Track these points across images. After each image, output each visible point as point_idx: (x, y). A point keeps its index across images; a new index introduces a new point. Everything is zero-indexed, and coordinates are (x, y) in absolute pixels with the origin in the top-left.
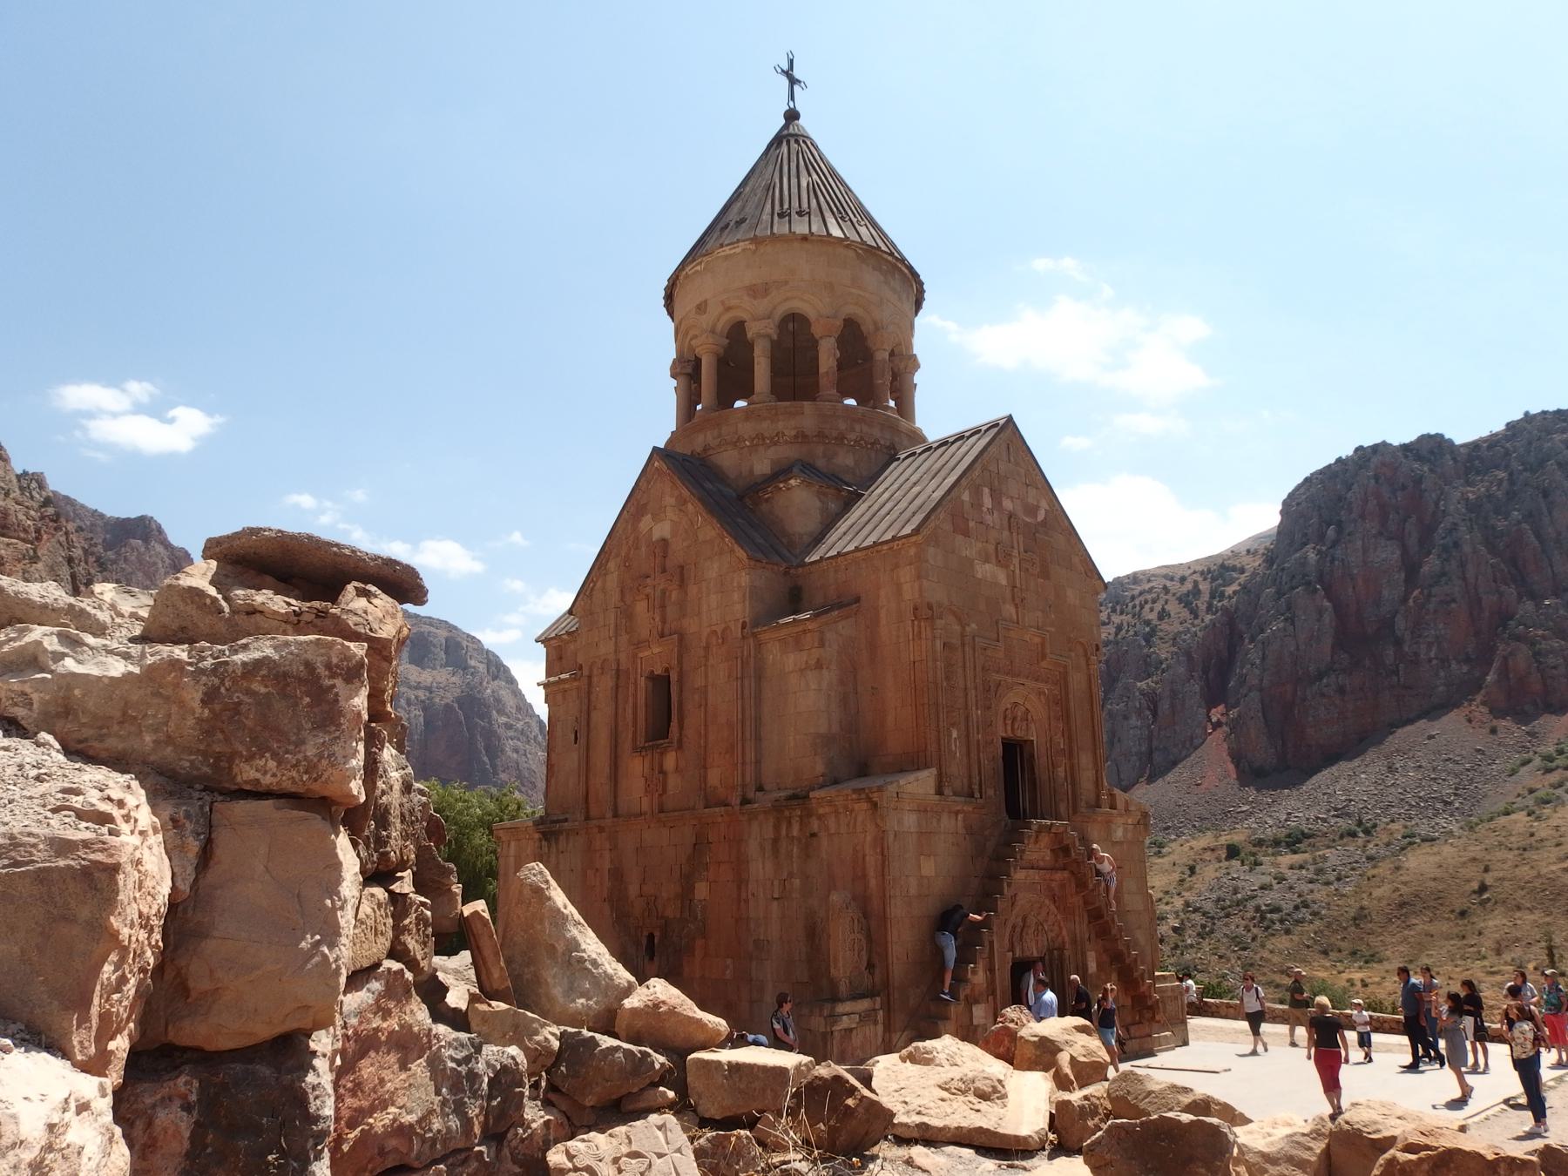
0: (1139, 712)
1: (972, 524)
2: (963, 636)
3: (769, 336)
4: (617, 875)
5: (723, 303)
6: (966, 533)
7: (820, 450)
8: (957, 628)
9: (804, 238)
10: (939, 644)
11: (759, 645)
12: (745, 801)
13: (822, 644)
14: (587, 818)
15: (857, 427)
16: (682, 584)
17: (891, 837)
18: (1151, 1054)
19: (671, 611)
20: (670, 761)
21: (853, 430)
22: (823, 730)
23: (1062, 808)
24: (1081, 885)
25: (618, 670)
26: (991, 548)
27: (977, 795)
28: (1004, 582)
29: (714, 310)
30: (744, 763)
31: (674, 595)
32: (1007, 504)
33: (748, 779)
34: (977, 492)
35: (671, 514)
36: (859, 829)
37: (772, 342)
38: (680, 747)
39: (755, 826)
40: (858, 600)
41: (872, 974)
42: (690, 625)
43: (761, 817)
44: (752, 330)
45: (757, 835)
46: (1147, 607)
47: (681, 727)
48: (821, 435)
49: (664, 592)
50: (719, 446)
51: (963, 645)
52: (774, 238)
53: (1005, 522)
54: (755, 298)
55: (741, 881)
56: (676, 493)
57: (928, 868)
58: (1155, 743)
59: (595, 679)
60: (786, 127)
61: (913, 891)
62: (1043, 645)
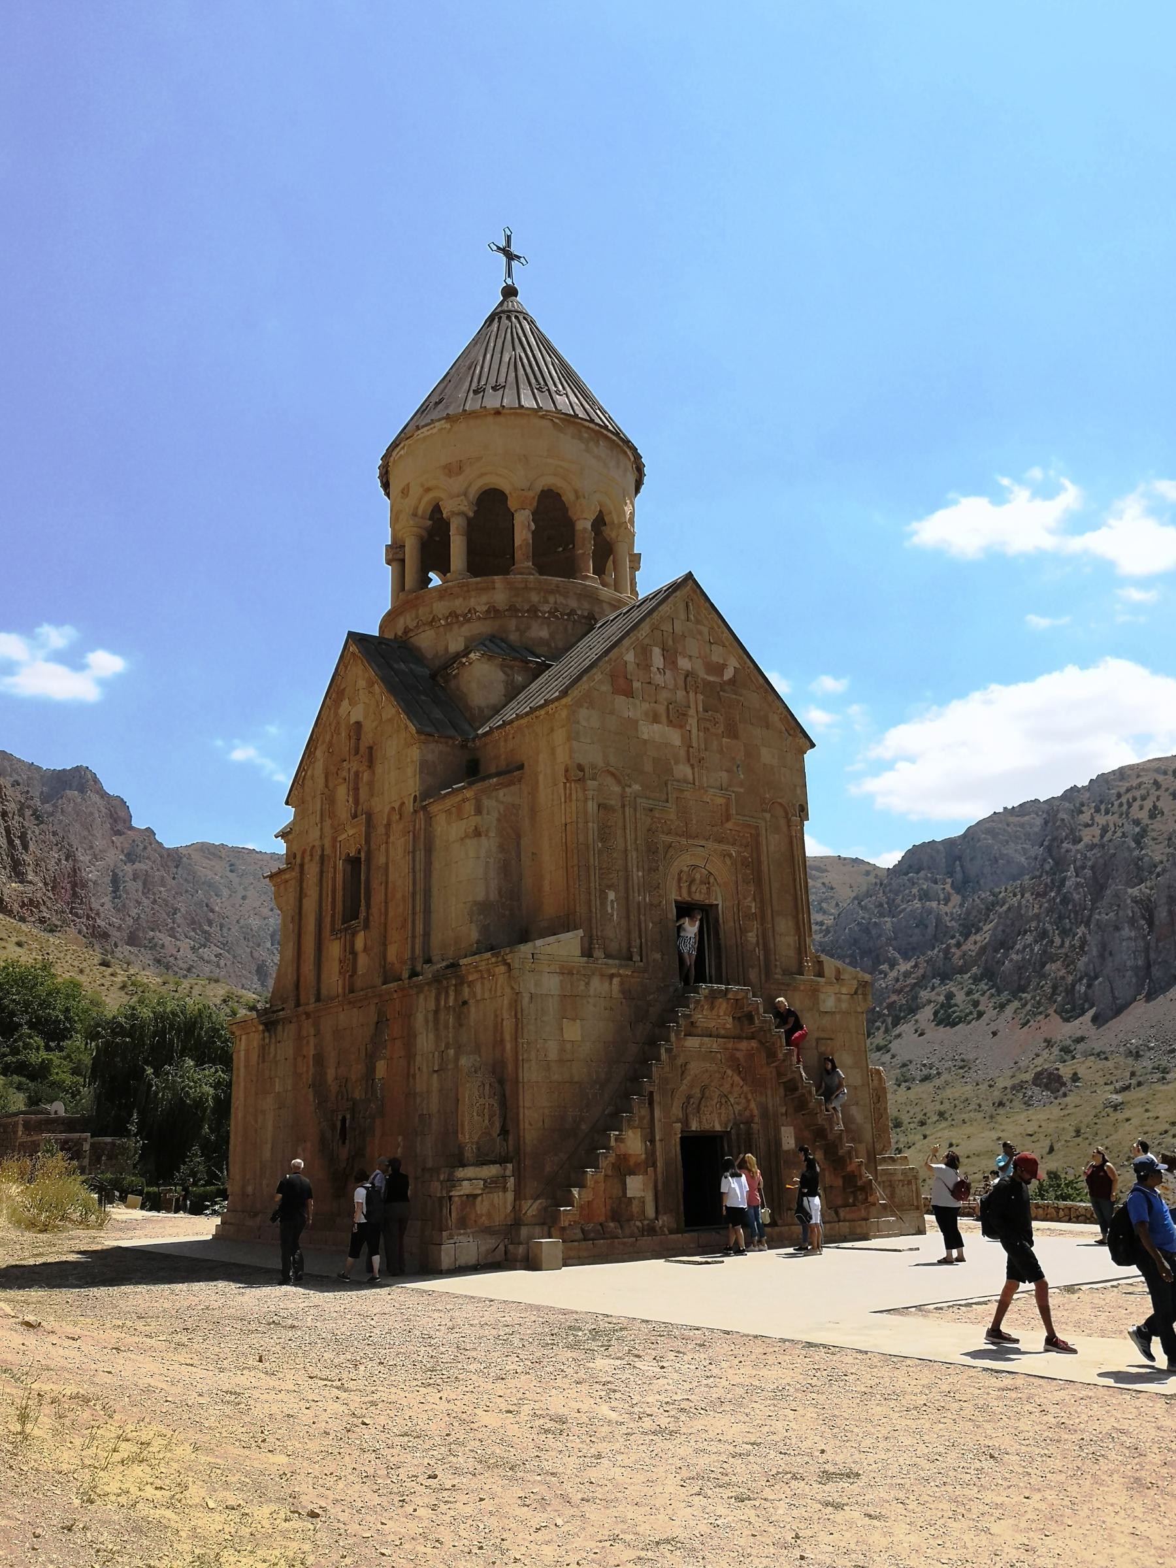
0: (1132, 922)
1: (636, 685)
2: (623, 797)
3: (463, 514)
4: (319, 1060)
5: (422, 485)
6: (629, 693)
7: (512, 624)
8: (617, 789)
9: (497, 413)
10: (591, 806)
11: (429, 819)
12: (414, 974)
13: (478, 811)
14: (298, 1005)
15: (551, 599)
16: (371, 764)
17: (526, 1000)
18: (865, 1238)
19: (363, 793)
21: (547, 602)
22: (480, 897)
23: (753, 975)
24: (771, 1055)
25: (322, 856)
26: (661, 709)
27: (637, 958)
28: (678, 743)
29: (416, 491)
30: (414, 937)
31: (366, 776)
32: (684, 663)
33: (417, 952)
34: (644, 652)
35: (363, 696)
36: (499, 994)
37: (470, 521)
38: (366, 926)
39: (422, 997)
40: (521, 767)
41: (506, 1140)
43: (426, 988)
45: (424, 1005)
46: (1136, 805)
47: (368, 907)
48: (513, 609)
49: (357, 774)
50: (417, 626)
51: (623, 806)
52: (467, 415)
55: (410, 1056)
56: (367, 675)
58: (1153, 956)
59: (306, 867)
60: (501, 304)
61: (553, 1055)
62: (727, 805)
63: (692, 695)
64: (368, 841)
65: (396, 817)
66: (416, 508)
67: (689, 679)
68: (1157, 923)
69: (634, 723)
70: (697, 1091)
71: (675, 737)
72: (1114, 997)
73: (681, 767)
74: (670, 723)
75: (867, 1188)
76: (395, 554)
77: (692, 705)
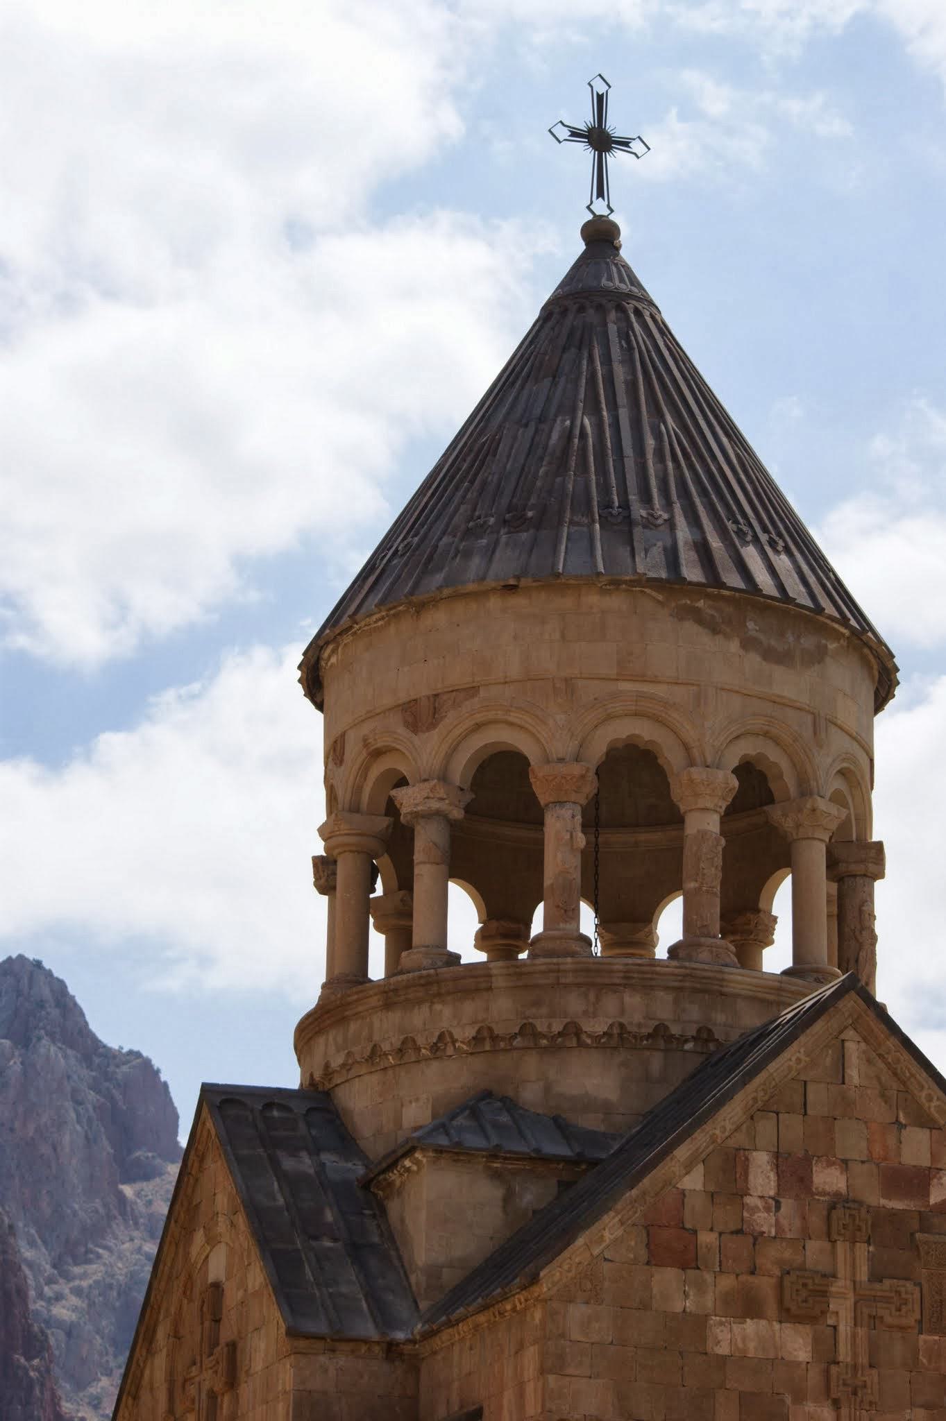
1: (707, 1238)
3: (438, 813)
5: (366, 743)
7: (531, 1065)
16: (232, 1382)
26: (765, 1285)
31: (226, 1402)
32: (828, 1179)
34: (729, 1172)
37: (453, 825)
48: (527, 1030)
53: (816, 1221)
54: (415, 725)
63: (841, 1248)
66: (358, 790)
67: (838, 1213)
69: (699, 1323)
73: (810, 1407)
77: (842, 1271)
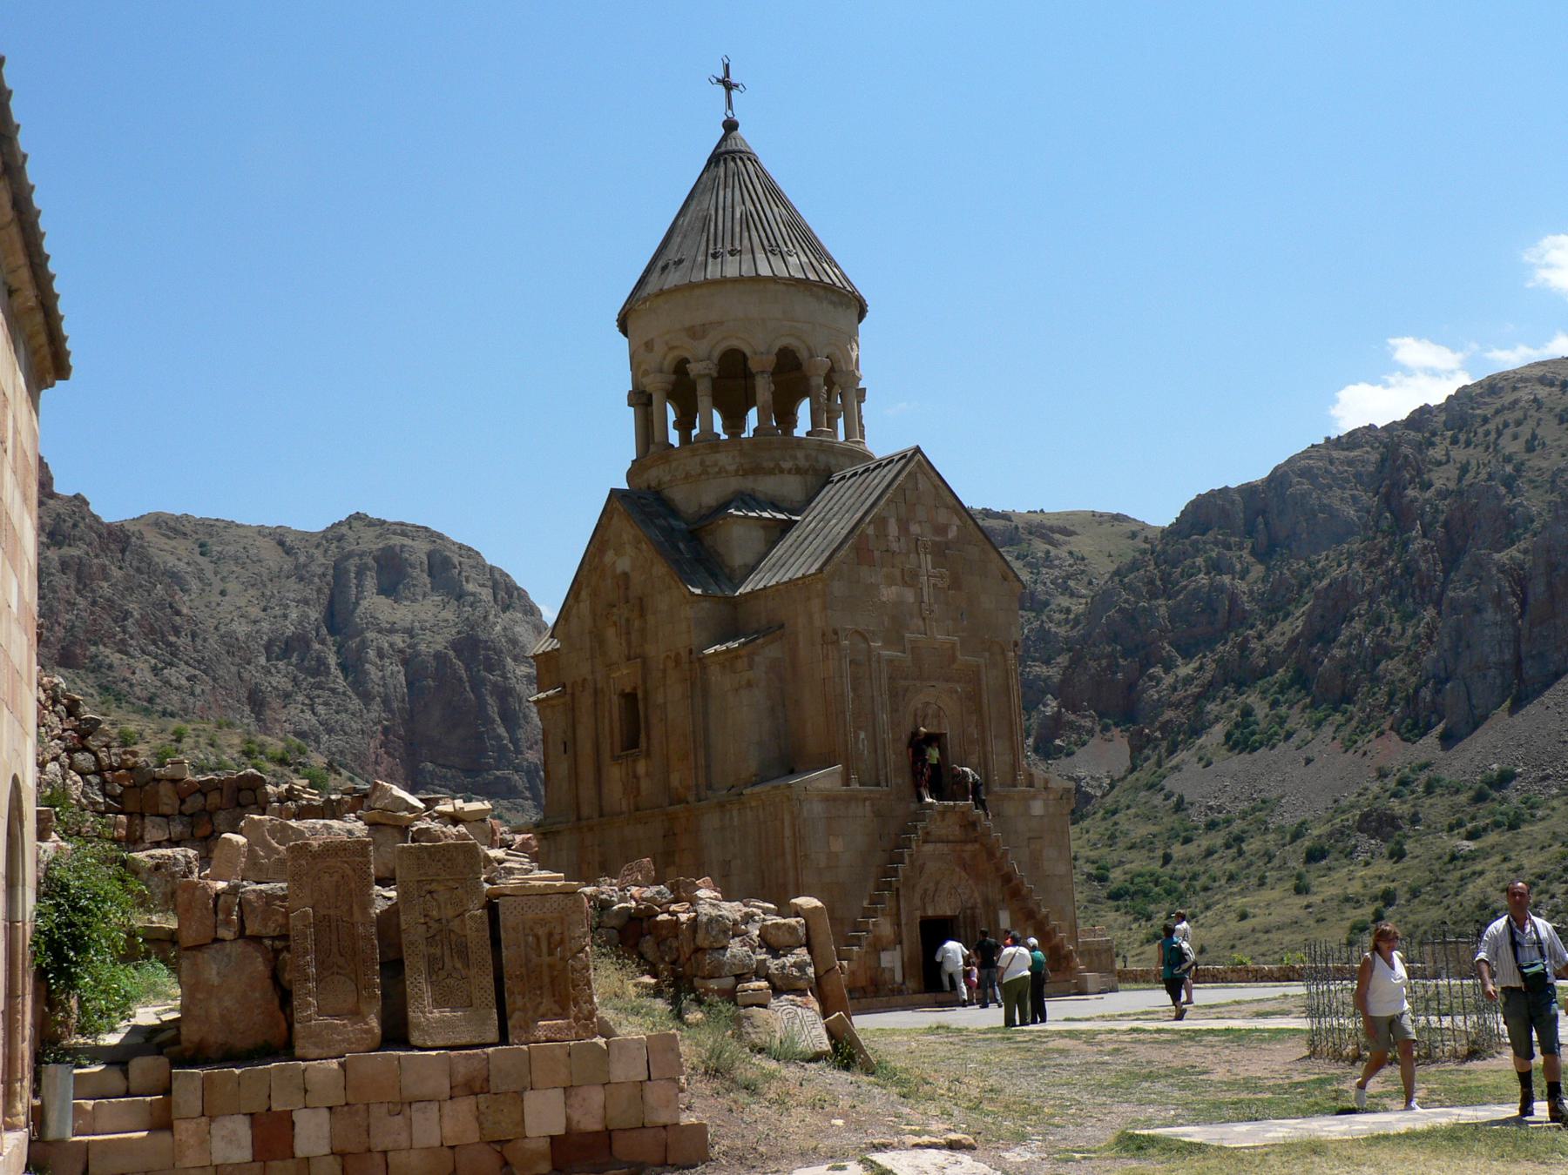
0: (1498, 599)
1: (877, 554)
6: (872, 564)
8: (864, 646)
14: (579, 819)
16: (642, 615)
20: (641, 767)
24: (991, 854)
26: (897, 572)
28: (911, 600)
29: (659, 349)
31: (637, 624)
35: (629, 549)
38: (648, 755)
40: (782, 626)
42: (651, 650)
44: (694, 368)
46: (1508, 432)
53: (912, 546)
57: (837, 845)
58: (1524, 648)
60: (724, 139)
61: (822, 865)
64: (644, 681)
65: (671, 664)
68: (1531, 600)
70: (931, 886)
71: (910, 596)
72: (1472, 707)
74: (905, 584)
75: (1068, 957)
76: (641, 399)
